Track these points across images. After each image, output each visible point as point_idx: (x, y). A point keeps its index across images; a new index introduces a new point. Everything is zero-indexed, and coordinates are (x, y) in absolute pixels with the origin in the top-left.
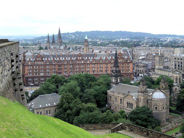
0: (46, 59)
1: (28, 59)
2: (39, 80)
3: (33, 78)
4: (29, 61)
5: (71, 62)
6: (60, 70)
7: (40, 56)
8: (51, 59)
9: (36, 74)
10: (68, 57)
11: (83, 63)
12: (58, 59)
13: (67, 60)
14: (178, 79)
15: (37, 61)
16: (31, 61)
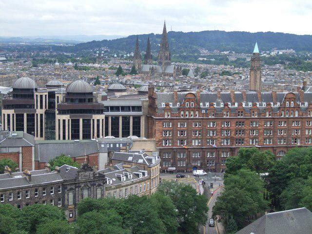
0: (207, 104)
1: (163, 105)
2: (189, 156)
3: (174, 151)
4: (164, 109)
5: (267, 113)
6: (241, 133)
7: (192, 97)
8: (218, 104)
9: (182, 142)
10: (262, 101)
11: (297, 116)
12: (236, 105)
13: (258, 109)
15: (184, 110)
16: (170, 110)
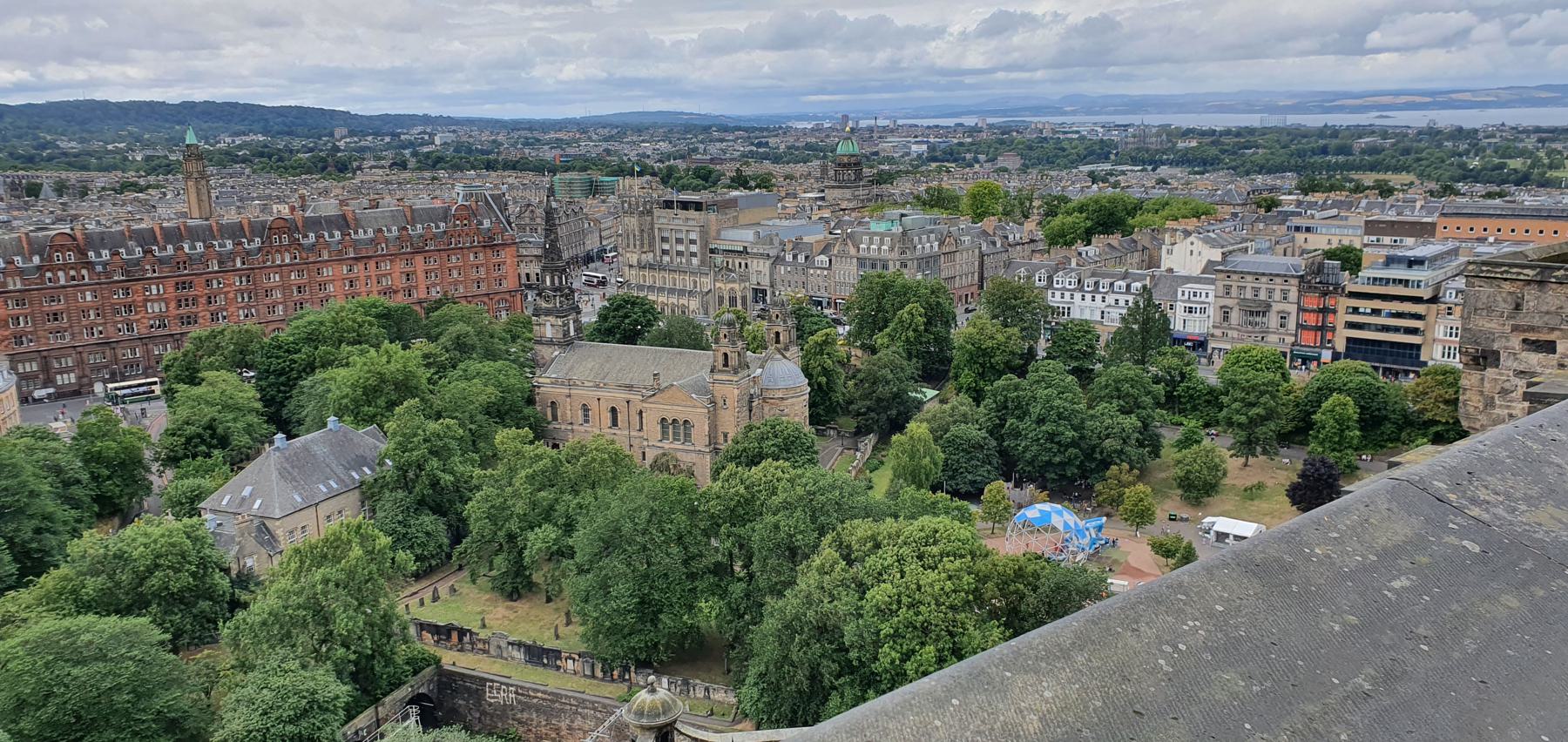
2: (80, 363)
10: (222, 237)
14: (739, 301)
